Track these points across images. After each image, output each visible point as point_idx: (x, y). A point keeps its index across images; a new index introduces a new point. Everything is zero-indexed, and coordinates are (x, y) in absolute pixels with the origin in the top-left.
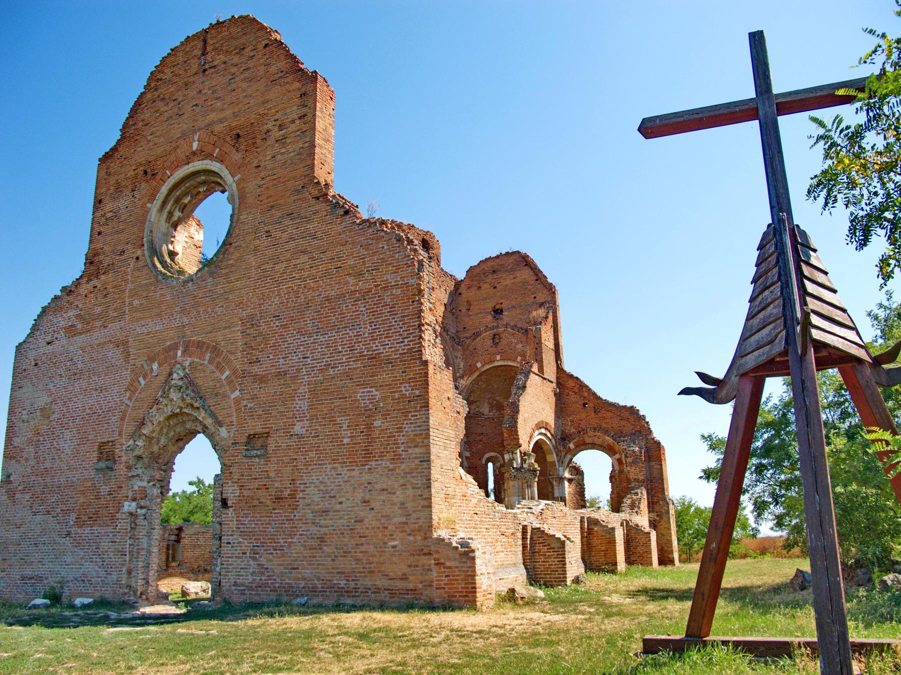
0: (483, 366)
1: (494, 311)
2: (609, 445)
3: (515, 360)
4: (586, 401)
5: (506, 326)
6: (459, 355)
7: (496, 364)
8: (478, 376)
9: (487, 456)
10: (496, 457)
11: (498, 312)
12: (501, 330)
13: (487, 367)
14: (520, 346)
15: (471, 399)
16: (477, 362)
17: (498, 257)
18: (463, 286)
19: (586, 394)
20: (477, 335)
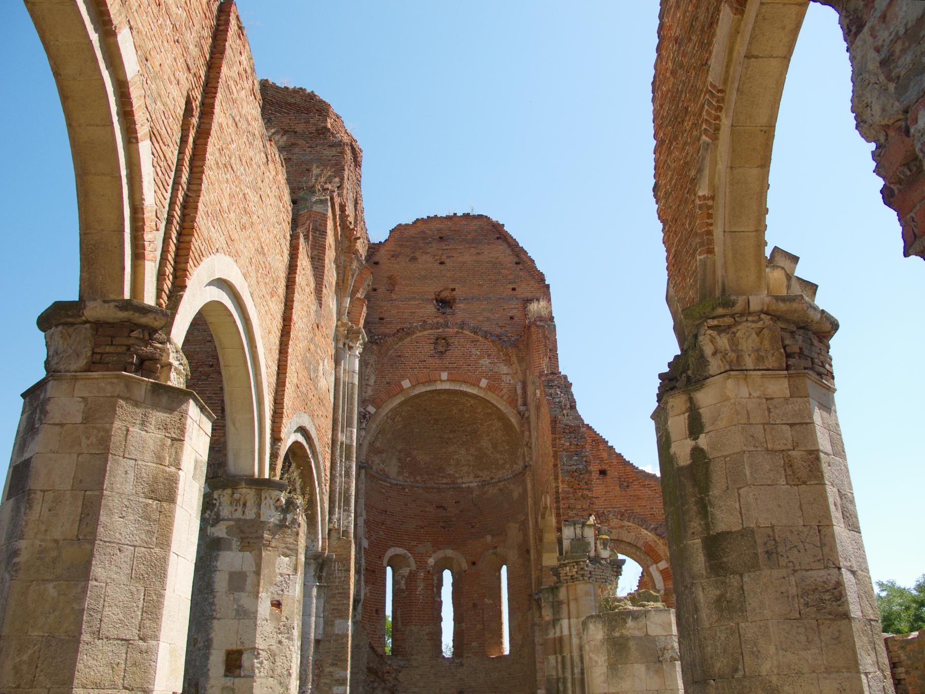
0: (413, 386)
1: (437, 301)
2: (646, 544)
3: (476, 384)
4: (604, 467)
5: (462, 326)
6: (372, 361)
7: (439, 386)
8: (401, 404)
9: (391, 552)
10: (404, 557)
11: (444, 303)
12: (451, 331)
13: (418, 391)
14: (485, 362)
15: (378, 444)
16: (403, 377)
17: (448, 218)
18: (383, 251)
19: (605, 455)
20: (404, 332)
